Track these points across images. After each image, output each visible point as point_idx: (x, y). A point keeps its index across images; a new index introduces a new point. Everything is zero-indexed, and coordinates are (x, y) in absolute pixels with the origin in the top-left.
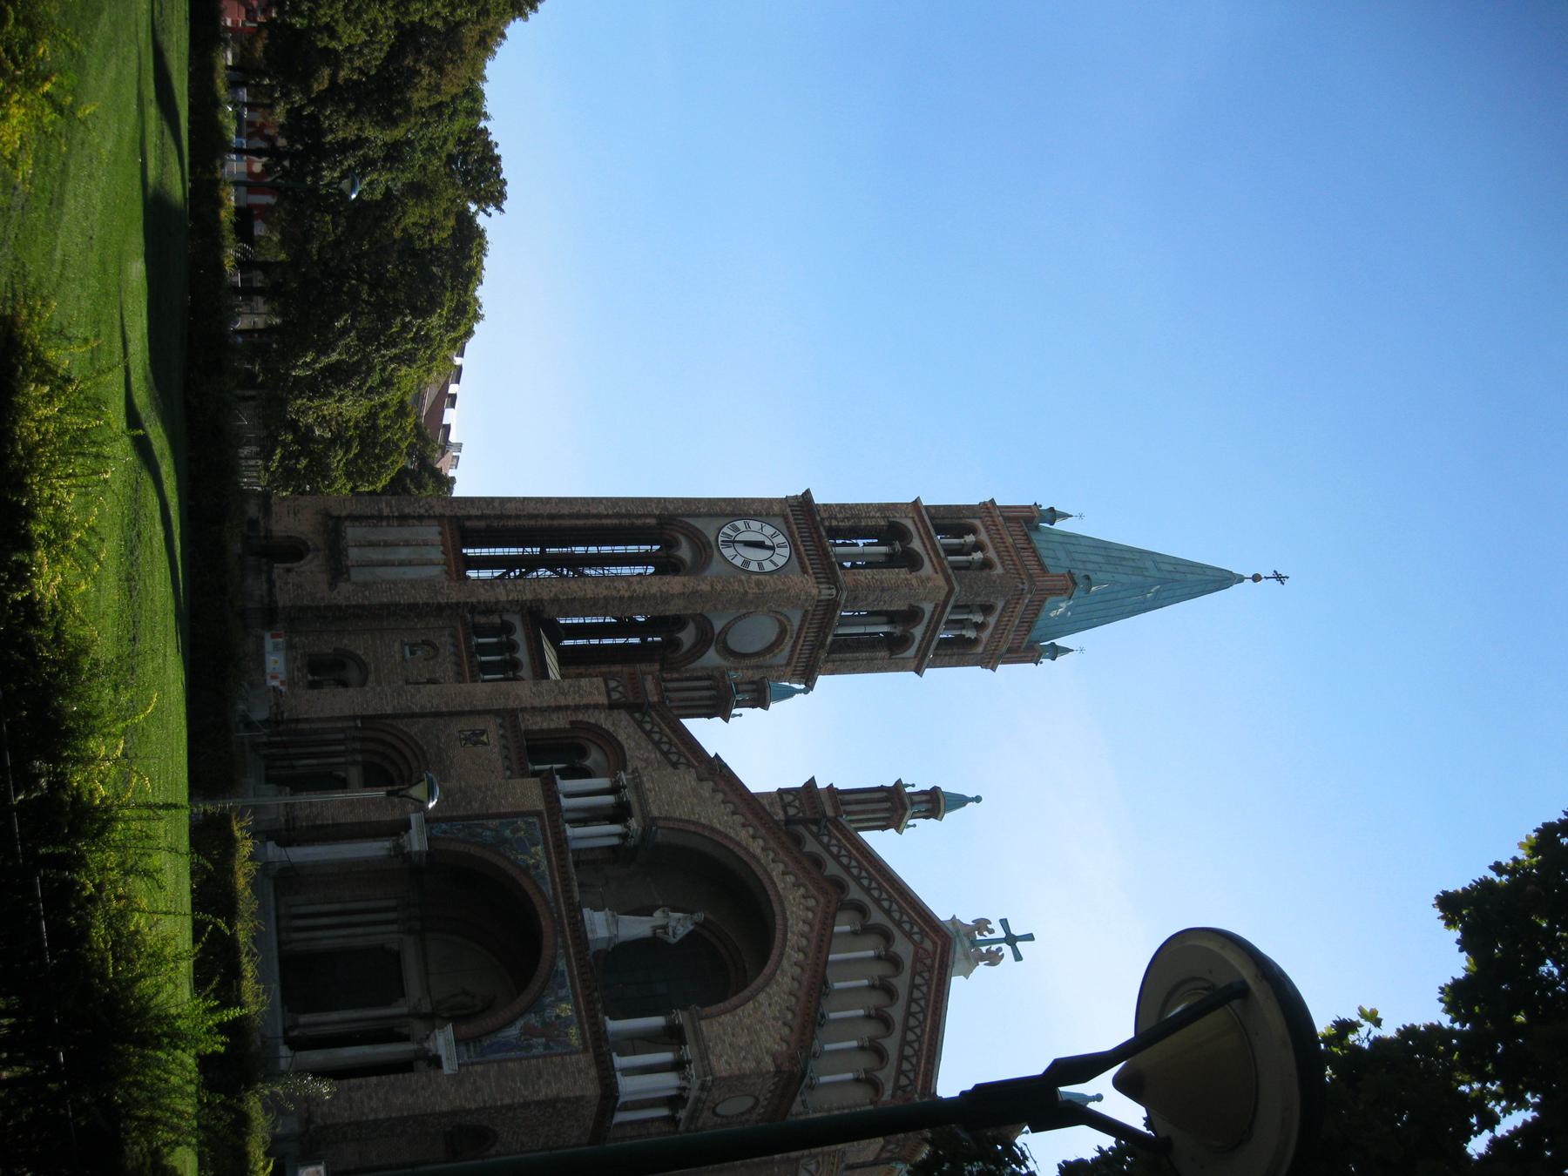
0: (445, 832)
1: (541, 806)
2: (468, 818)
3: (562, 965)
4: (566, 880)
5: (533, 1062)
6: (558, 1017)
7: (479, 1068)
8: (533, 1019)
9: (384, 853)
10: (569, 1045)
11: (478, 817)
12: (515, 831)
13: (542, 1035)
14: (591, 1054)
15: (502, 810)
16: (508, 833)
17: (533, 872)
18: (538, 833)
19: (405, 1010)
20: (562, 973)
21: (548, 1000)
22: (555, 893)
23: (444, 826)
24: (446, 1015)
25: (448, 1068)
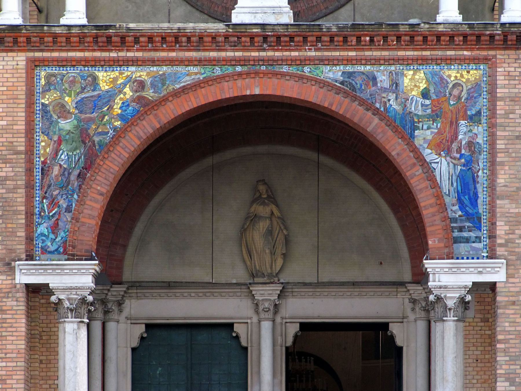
0: (55, 228)
1: (19, 60)
2: (29, 186)
3: (333, 73)
4: (176, 40)
5: (500, 145)
6: (425, 95)
7: (501, 228)
8: (424, 135)
9: (83, 333)
10: (477, 86)
11: (29, 171)
12: (63, 111)
13: (454, 125)
14: (500, 55)
15: (21, 126)
16: (66, 125)
17: (150, 94)
18: (72, 72)
19: (266, 326)
20: (350, 75)
21: (394, 105)
22: (200, 62)
23: (43, 229)
24: (280, 262)
25: (497, 275)
